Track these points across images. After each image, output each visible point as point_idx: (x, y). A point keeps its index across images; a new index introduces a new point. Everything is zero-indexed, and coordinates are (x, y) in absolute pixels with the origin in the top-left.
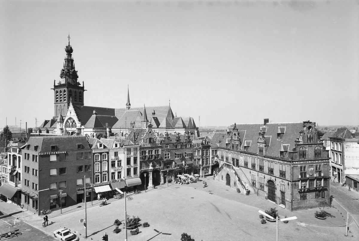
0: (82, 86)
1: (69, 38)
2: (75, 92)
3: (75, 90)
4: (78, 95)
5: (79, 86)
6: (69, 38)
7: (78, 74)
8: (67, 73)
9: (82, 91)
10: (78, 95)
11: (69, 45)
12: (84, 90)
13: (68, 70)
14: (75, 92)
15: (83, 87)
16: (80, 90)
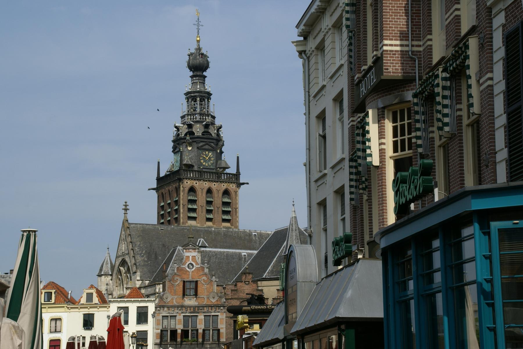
0: (232, 170)
1: (198, 25)
2: (209, 191)
3: (206, 185)
4: (218, 199)
5: (227, 171)
6: (198, 25)
7: (223, 133)
8: (186, 135)
9: (232, 187)
10: (218, 199)
11: (199, 49)
12: (239, 185)
13: (190, 126)
14: (209, 191)
15: (237, 175)
16: (224, 186)
